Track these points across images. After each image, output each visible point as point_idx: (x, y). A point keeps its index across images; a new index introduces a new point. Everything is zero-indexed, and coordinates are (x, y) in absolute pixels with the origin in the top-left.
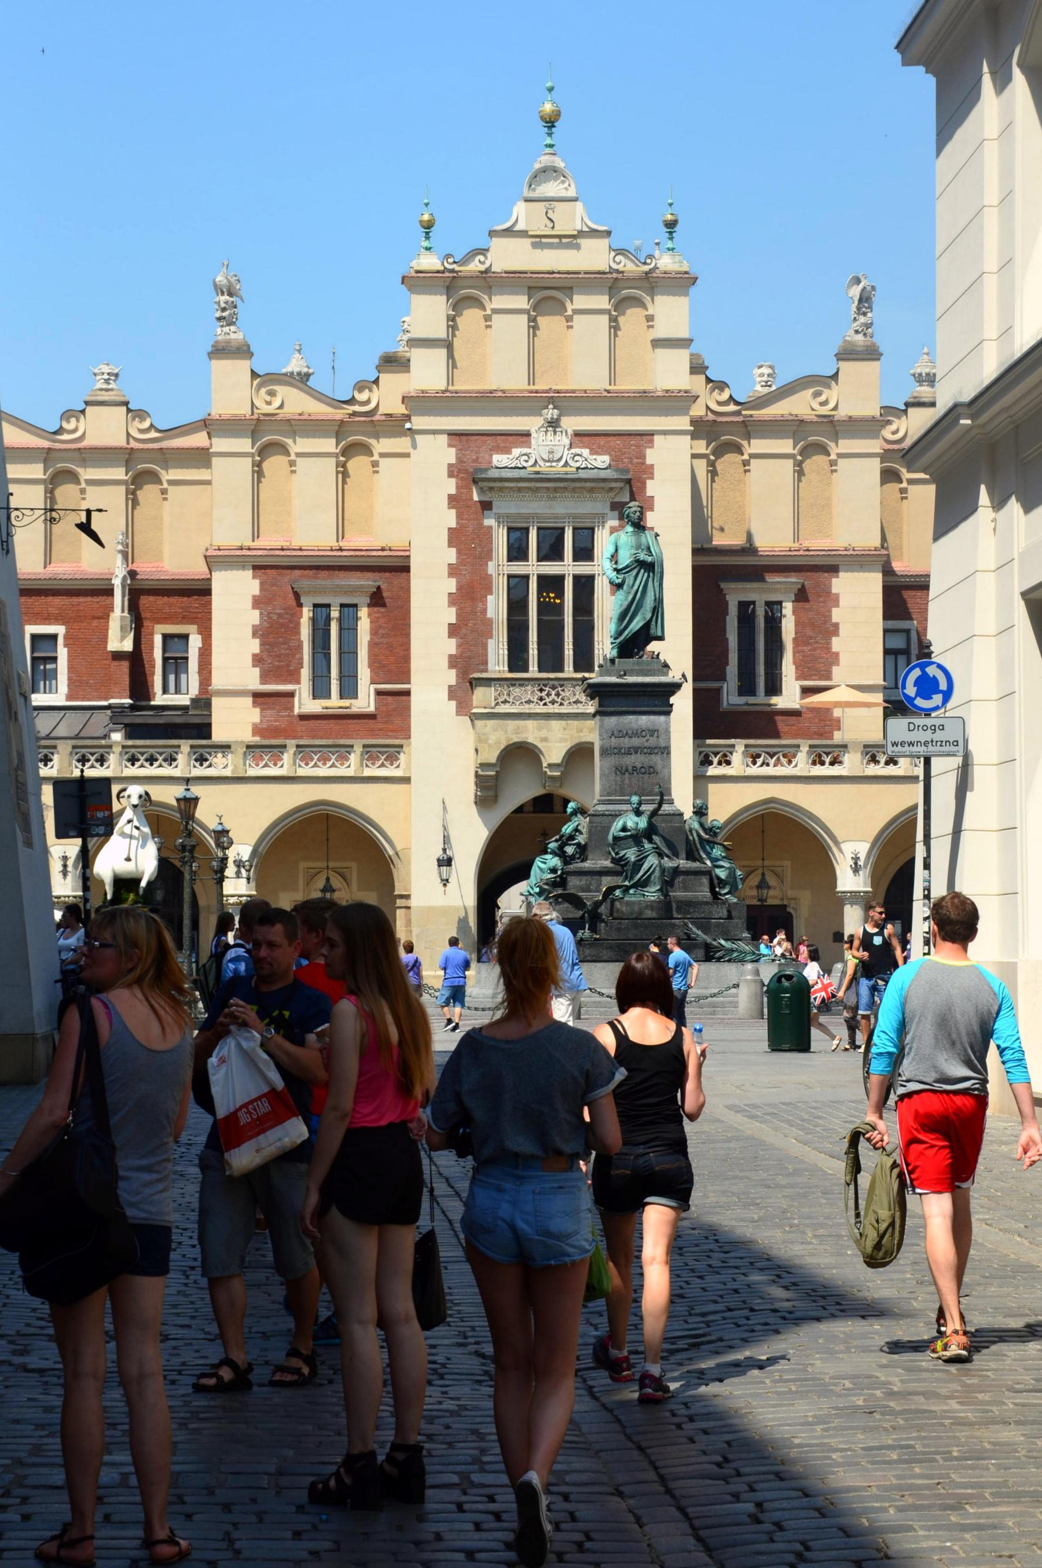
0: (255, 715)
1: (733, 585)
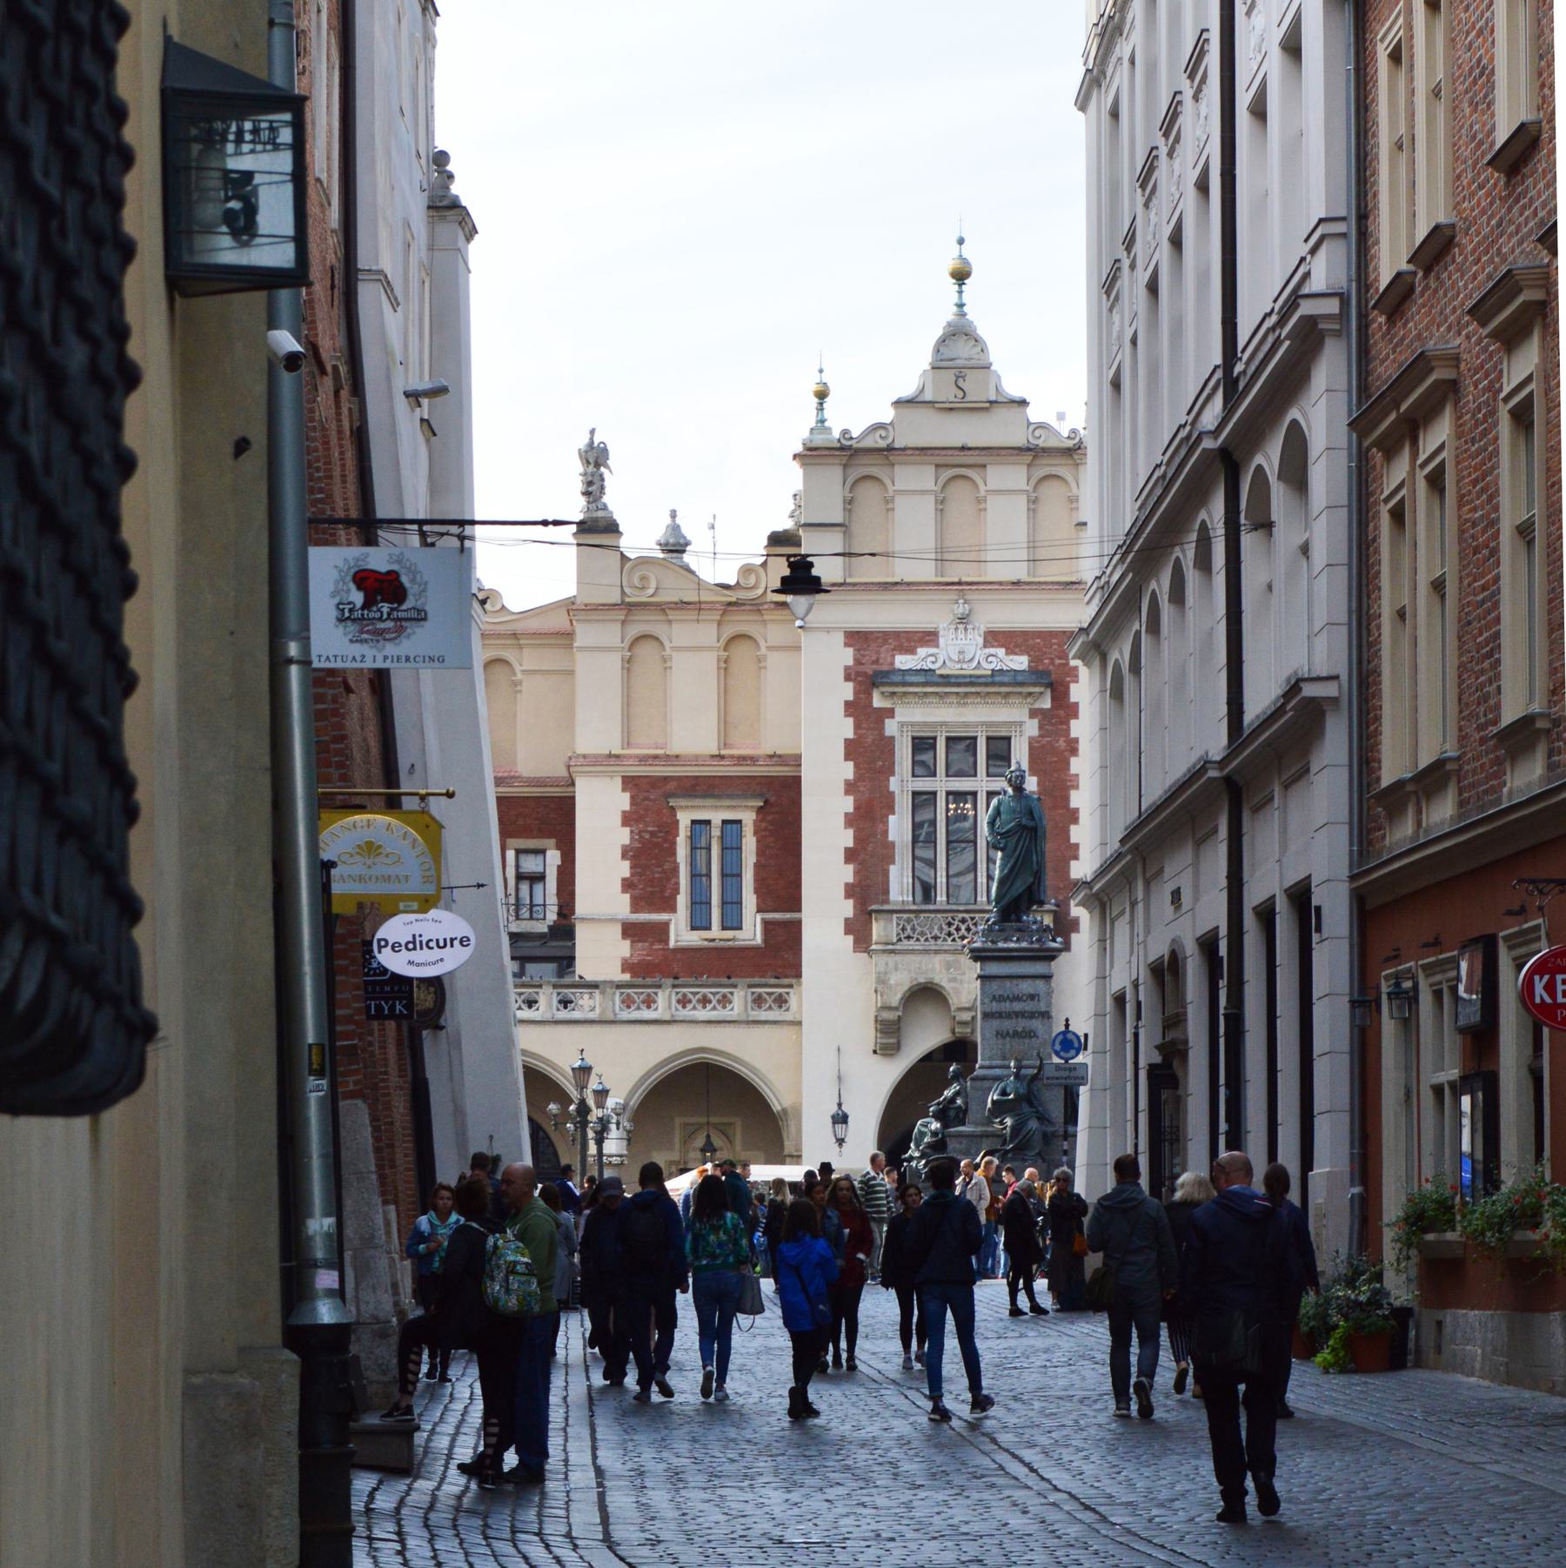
0: (624, 949)
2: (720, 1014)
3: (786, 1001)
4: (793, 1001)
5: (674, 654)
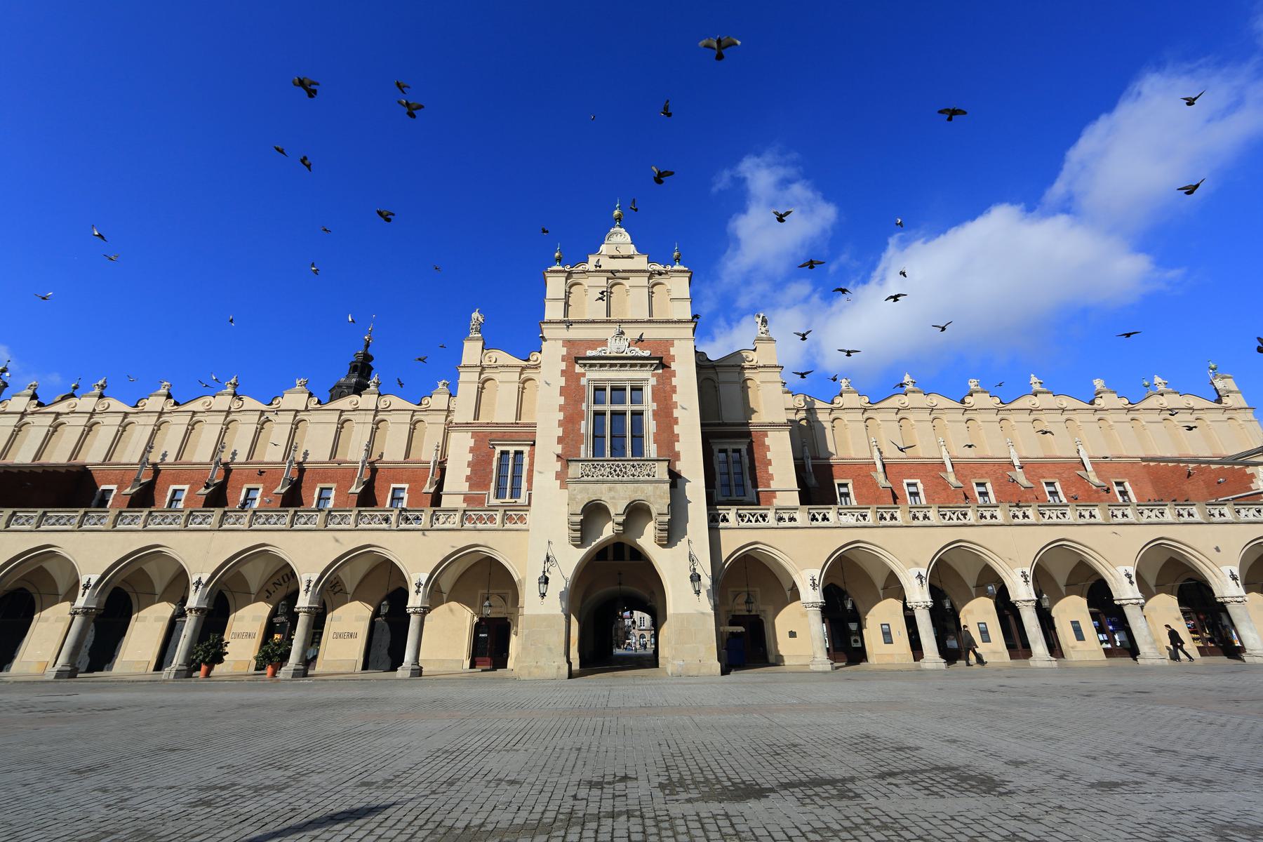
2: (489, 525)
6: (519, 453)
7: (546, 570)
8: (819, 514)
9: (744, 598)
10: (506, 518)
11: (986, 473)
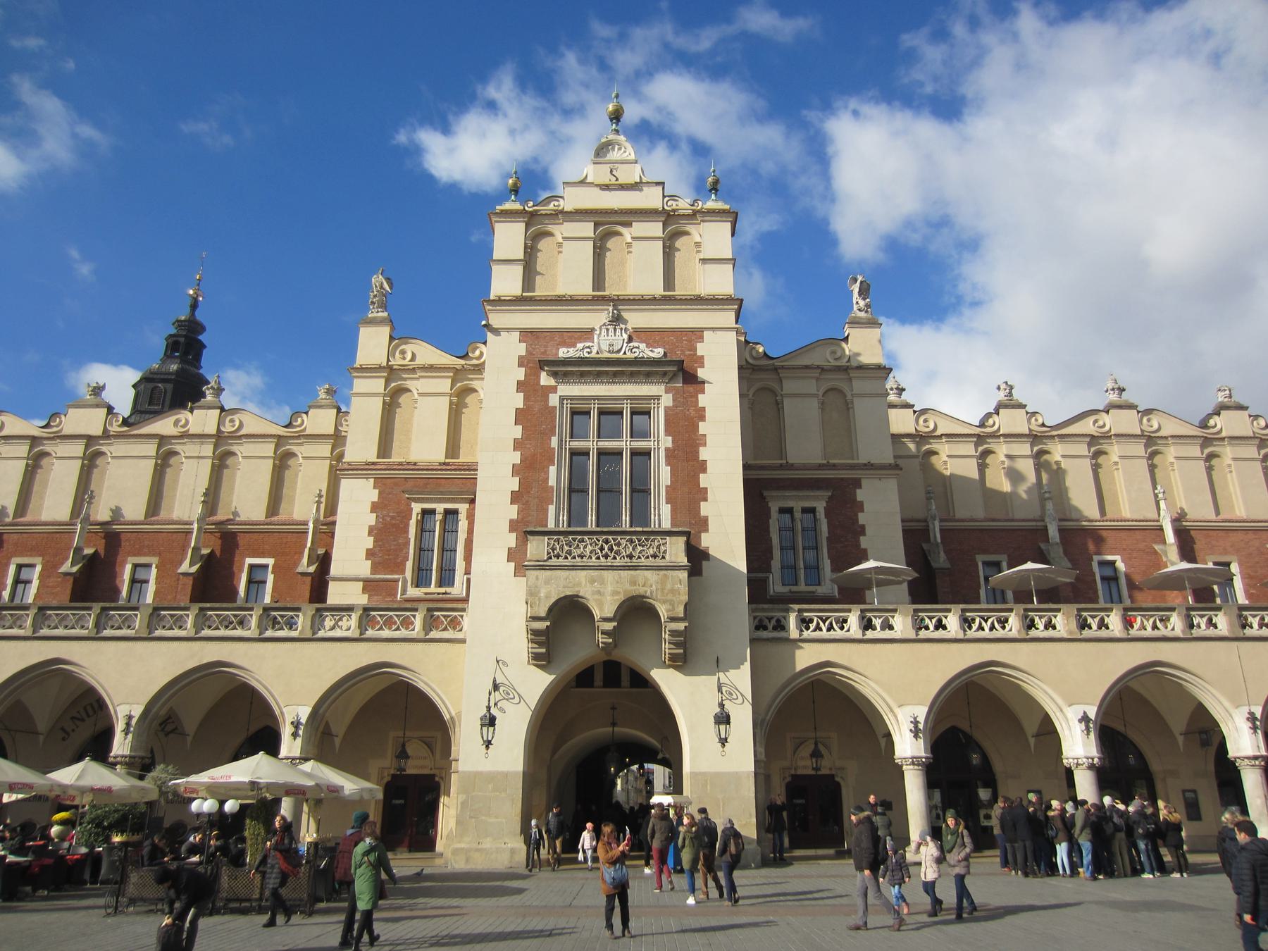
1: (774, 493)
2: (403, 633)
3: (459, 623)
4: (466, 623)
5: (420, 399)
6: (451, 514)
7: (492, 704)
8: (931, 618)
9: (808, 749)
10: (430, 624)
11: (1231, 547)
